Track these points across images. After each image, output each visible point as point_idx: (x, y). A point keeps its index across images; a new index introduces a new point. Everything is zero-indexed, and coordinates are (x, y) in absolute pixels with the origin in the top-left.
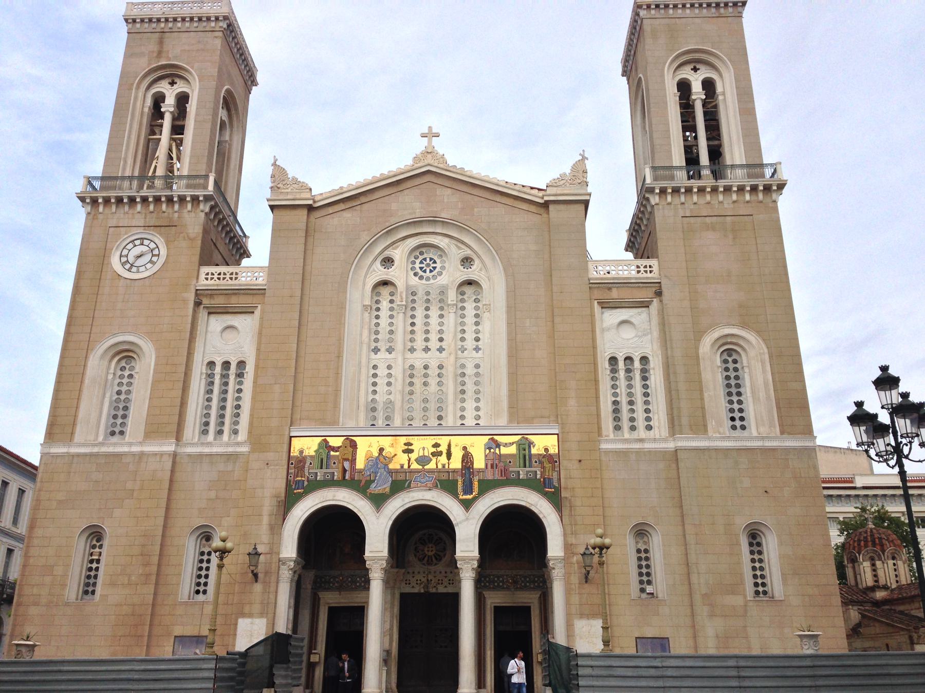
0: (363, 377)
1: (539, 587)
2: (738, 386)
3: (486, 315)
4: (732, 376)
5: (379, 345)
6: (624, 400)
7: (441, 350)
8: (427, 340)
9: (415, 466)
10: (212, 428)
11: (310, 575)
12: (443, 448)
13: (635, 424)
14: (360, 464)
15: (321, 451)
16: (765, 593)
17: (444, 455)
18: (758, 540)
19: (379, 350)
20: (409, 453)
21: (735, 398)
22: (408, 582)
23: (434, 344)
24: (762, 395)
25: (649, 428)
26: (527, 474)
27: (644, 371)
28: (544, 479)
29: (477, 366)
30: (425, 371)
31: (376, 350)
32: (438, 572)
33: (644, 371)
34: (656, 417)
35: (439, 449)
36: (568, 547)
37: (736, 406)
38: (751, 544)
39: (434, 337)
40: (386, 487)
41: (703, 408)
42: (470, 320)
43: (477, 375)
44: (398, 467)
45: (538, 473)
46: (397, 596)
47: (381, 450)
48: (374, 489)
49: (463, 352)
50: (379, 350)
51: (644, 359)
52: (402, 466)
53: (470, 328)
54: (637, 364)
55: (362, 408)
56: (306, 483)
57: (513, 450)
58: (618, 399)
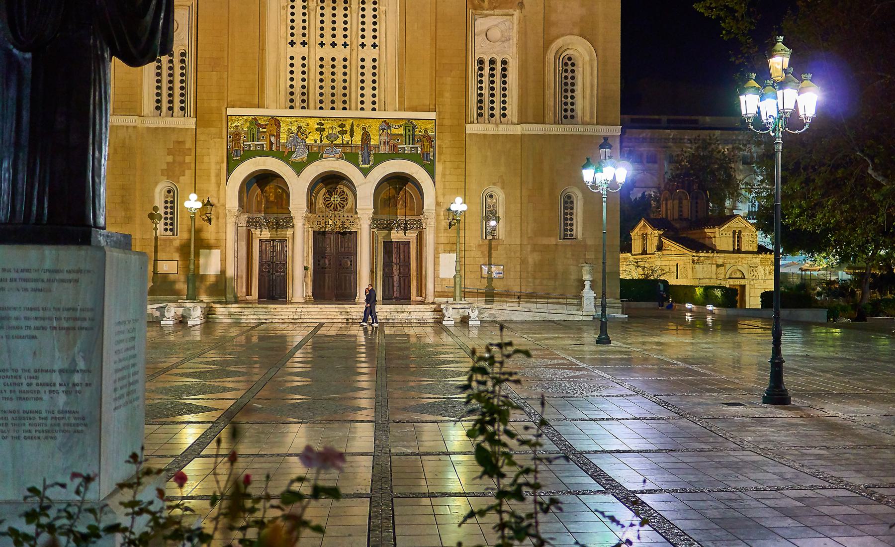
0: (282, 68)
1: (416, 228)
2: (573, 84)
3: (383, 16)
4: (569, 77)
5: (294, 38)
6: (485, 92)
7: (345, 45)
8: (334, 36)
9: (325, 141)
10: (165, 105)
11: (245, 216)
12: (348, 128)
13: (494, 112)
14: (283, 138)
15: (252, 127)
16: (571, 236)
17: (348, 133)
18: (572, 200)
19: (295, 43)
20: (321, 131)
21: (569, 94)
22: (319, 223)
23: (340, 40)
24: (588, 92)
25: (504, 115)
26: (411, 151)
27: (504, 69)
28: (423, 154)
29: (374, 60)
30: (333, 63)
31: (292, 43)
32: (342, 217)
33: (504, 69)
34: (510, 108)
35: (344, 129)
36: (438, 204)
37: (569, 100)
38: (566, 203)
39: (340, 33)
40: (304, 157)
41: (544, 103)
42: (369, 19)
43: (374, 67)
44: (313, 142)
45: (419, 149)
46: (311, 233)
47: (299, 128)
48: (295, 158)
49: (363, 48)
50: (295, 43)
51: (504, 62)
52: (316, 141)
53: (369, 27)
54: (499, 67)
55: (283, 93)
56: (242, 152)
57: (400, 131)
58: (483, 92)
